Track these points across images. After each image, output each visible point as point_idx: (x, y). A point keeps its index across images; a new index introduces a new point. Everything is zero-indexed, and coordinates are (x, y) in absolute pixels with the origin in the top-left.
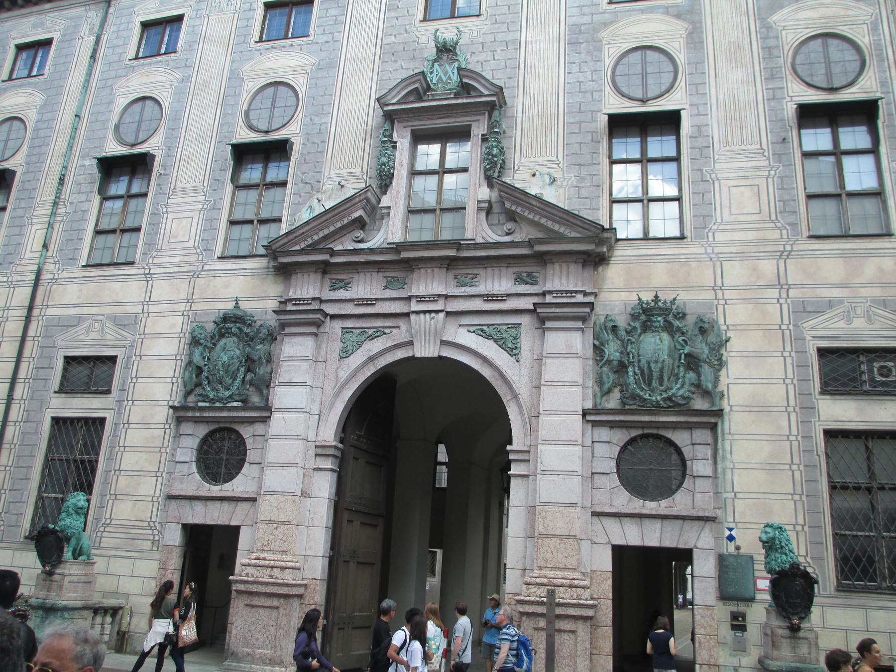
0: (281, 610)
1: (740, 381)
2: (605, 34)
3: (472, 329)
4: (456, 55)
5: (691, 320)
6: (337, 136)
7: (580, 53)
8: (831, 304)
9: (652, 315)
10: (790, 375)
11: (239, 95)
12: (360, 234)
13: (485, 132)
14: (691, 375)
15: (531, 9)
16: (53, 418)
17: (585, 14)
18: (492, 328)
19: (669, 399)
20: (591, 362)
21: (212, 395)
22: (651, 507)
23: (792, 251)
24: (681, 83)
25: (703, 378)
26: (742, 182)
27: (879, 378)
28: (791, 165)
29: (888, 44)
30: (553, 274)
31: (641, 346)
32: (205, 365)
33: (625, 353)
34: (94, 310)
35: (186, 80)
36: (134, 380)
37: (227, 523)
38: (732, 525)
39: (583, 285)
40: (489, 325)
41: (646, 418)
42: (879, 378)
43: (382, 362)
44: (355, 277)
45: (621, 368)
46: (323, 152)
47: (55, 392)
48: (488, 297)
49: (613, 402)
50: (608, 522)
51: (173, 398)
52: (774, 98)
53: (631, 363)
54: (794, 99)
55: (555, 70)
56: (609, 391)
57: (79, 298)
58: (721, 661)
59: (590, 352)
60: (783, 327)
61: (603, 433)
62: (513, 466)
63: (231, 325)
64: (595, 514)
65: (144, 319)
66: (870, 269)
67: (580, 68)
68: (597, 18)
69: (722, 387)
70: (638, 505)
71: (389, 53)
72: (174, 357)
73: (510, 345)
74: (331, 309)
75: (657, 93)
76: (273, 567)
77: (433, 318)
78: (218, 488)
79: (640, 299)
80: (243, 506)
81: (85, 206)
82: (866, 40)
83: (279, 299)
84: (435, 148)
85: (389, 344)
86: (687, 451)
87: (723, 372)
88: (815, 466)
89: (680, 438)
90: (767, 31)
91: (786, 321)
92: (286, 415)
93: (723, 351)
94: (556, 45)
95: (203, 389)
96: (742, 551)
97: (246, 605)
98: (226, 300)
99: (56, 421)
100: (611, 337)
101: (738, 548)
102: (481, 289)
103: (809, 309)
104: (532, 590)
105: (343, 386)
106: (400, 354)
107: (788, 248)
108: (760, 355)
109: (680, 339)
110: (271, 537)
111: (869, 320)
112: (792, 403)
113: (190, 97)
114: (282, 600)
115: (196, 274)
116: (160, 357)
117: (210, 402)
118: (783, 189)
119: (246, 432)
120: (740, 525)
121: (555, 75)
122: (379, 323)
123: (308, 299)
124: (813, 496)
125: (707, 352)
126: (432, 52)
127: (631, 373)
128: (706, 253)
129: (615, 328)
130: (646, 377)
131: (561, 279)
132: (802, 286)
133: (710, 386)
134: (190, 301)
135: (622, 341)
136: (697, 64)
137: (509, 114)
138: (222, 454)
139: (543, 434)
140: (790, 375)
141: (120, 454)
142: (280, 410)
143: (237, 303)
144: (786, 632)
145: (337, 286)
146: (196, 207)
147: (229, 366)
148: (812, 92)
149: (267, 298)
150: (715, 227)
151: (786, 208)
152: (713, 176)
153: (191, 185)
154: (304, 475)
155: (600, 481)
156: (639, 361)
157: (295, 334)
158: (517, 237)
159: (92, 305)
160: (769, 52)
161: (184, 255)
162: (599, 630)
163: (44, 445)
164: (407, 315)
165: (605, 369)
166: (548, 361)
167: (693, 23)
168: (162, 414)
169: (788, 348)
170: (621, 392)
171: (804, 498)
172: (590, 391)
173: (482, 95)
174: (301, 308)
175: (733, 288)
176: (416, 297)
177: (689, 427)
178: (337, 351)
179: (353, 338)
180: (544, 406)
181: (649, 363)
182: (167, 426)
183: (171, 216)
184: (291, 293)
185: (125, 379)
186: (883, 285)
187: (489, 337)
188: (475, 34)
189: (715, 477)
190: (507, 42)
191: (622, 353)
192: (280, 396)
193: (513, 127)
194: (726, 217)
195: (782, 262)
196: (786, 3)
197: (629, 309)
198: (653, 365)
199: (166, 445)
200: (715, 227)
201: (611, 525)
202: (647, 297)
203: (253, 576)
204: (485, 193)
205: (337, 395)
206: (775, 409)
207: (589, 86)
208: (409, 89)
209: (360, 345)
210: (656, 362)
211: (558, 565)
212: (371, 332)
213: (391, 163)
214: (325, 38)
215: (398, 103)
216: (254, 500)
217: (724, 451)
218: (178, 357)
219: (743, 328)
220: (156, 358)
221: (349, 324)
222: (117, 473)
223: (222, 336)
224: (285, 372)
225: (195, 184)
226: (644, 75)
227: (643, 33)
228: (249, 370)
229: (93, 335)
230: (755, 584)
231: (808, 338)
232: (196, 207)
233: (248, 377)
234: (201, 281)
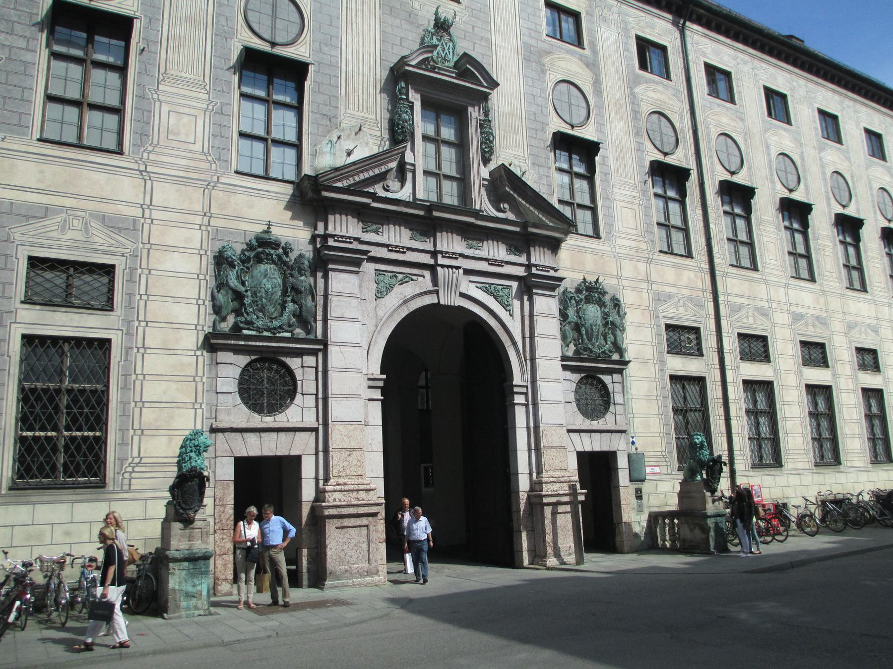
2: (546, 60)
3: (478, 285)
6: (349, 75)
8: (670, 296)
9: (591, 291)
16: (24, 336)
18: (492, 287)
34: (68, 202)
37: (287, 454)
46: (338, 87)
47: (22, 302)
50: (574, 436)
51: (202, 322)
55: (517, 78)
57: (39, 181)
62: (516, 396)
63: (272, 252)
65: (146, 227)
70: (588, 424)
76: (358, 491)
79: (584, 279)
81: (28, 57)
85: (418, 291)
90: (634, 99)
98: (252, 221)
99: (28, 340)
102: (483, 254)
108: (640, 326)
110: (346, 464)
111: (686, 310)
114: (370, 518)
115: (210, 186)
116: (176, 274)
117: (257, 331)
121: (518, 82)
123: (350, 238)
132: (657, 283)
134: (207, 214)
136: (600, 107)
138: (267, 385)
141: (138, 383)
142: (336, 344)
143: (269, 228)
145: (369, 229)
147: (272, 294)
153: (187, 75)
159: (64, 195)
161: (192, 159)
163: (15, 370)
167: (596, 74)
168: (191, 340)
175: (627, 279)
181: (591, 325)
183: (165, 108)
185: (131, 295)
187: (491, 294)
190: (482, 38)
192: (338, 331)
194: (621, 229)
199: (200, 373)
202: (591, 279)
203: (340, 501)
207: (540, 101)
209: (390, 288)
215: (417, 66)
218: (201, 277)
220: (171, 274)
223: (259, 260)
224: (336, 307)
225: (192, 76)
227: (569, 70)
229: (70, 235)
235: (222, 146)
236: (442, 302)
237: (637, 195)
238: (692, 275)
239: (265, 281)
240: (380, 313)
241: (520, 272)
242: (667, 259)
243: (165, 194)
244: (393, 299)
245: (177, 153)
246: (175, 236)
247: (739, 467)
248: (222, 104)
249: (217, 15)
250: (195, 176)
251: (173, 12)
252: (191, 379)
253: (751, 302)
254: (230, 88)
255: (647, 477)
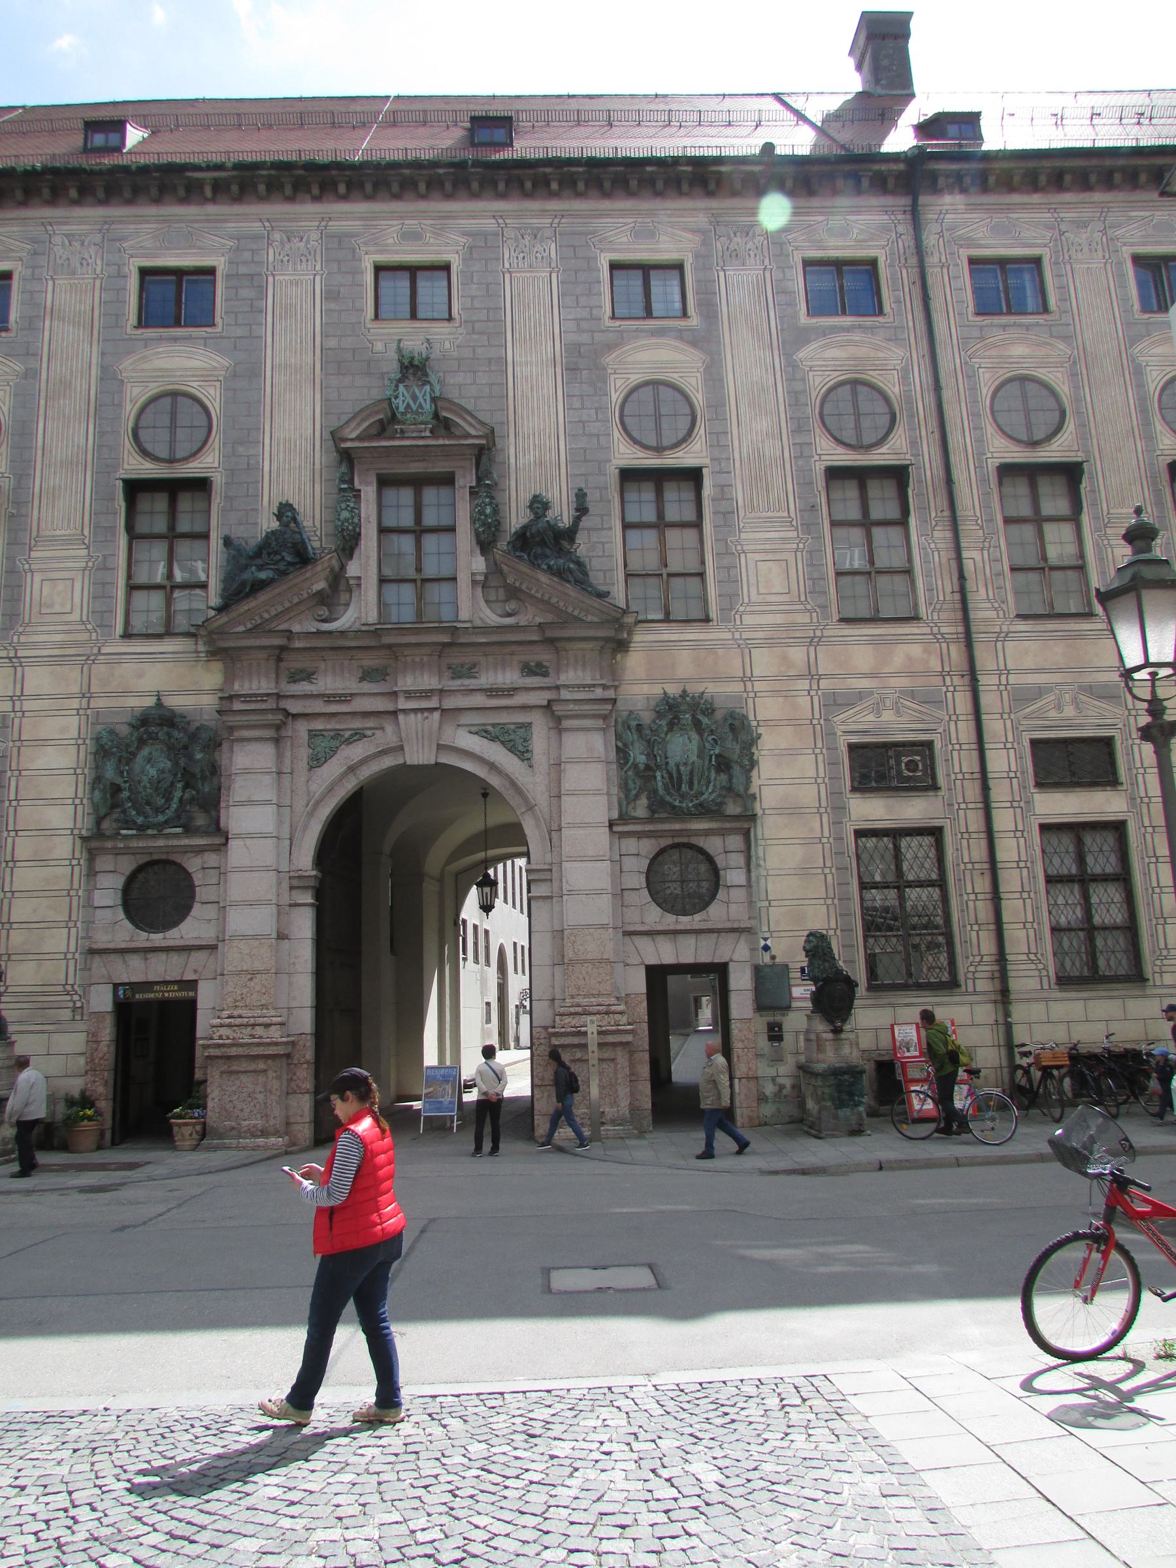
0: (271, 1074)
1: (772, 782)
4: (427, 375)
5: (719, 715)
6: (274, 475)
7: (581, 383)
8: (861, 695)
9: (678, 711)
10: (822, 774)
11: (120, 405)
12: (324, 612)
13: (474, 484)
14: (724, 777)
15: (516, 317)
17: (583, 331)
18: (497, 729)
19: (701, 805)
20: (614, 766)
21: (140, 820)
22: (685, 921)
23: (822, 637)
24: (700, 431)
25: (734, 780)
26: (770, 556)
27: (906, 773)
28: (819, 538)
29: (919, 396)
30: (567, 665)
31: (669, 746)
32: (125, 782)
33: (651, 755)
35: (31, 374)
36: (14, 803)
38: (767, 935)
39: (602, 678)
40: (493, 725)
41: (677, 826)
42: (906, 773)
43: (366, 772)
44: (322, 666)
45: (646, 774)
48: (492, 692)
49: (641, 809)
52: (801, 456)
53: (658, 767)
54: (824, 457)
56: (637, 797)
58: (760, 1073)
59: (613, 755)
60: (815, 722)
61: (630, 845)
64: (627, 934)
65: (17, 721)
66: (900, 655)
67: (582, 404)
68: (598, 337)
69: (754, 789)
71: (335, 363)
72: (72, 771)
73: (521, 748)
74: (294, 707)
75: (674, 441)
76: (254, 1025)
77: (427, 718)
78: (161, 935)
79: (665, 693)
80: (198, 958)
82: (896, 390)
83: (220, 695)
84: (406, 495)
85: (373, 750)
86: (720, 861)
87: (754, 773)
88: (846, 868)
89: (713, 845)
91: (817, 716)
92: (248, 842)
93: (754, 750)
94: (551, 370)
95: (124, 812)
96: (777, 960)
97: (222, 1073)
98: (141, 694)
100: (635, 737)
101: (773, 957)
103: (839, 702)
104: (567, 1021)
105: (318, 803)
106: (388, 762)
107: (818, 633)
109: (710, 738)
110: (245, 991)
111: (898, 713)
112: (824, 804)
113: (42, 402)
114: (269, 1062)
115: (90, 660)
118: (812, 565)
119: (193, 864)
120: (774, 935)
122: (357, 724)
124: (844, 899)
125: (738, 751)
126: (392, 367)
127: (659, 778)
128: (733, 639)
129: (639, 727)
130: (674, 782)
131: (575, 669)
132: (832, 676)
133: (741, 789)
134: (86, 695)
135: (648, 741)
137: (499, 459)
138: (158, 895)
139: (566, 849)
140: (822, 774)
142: (239, 836)
143: (159, 699)
144: (830, 1036)
145: (297, 677)
146: (77, 565)
147: (159, 782)
148: (840, 450)
149: (199, 692)
150: (741, 609)
151: (815, 587)
152: (739, 548)
153: (63, 532)
154: (279, 913)
155: (630, 897)
156: (667, 763)
157: (249, 740)
158: (522, 619)
160: (796, 399)
162: (636, 1056)
164: (394, 713)
165: (630, 773)
166: (568, 766)
168: (64, 847)
169: (819, 745)
170: (648, 798)
171: (836, 901)
172: (615, 799)
173: (468, 436)
174: (253, 706)
175: (763, 679)
176: (405, 692)
177: (722, 833)
178: (305, 760)
179: (322, 744)
180: (565, 820)
181: (678, 766)
182: (75, 862)
183: (38, 578)
184: (236, 687)
186: (911, 674)
188: (447, 345)
189: (749, 885)
191: (648, 755)
193: (505, 475)
194: (754, 597)
195: (812, 649)
196: (813, 337)
197: (653, 703)
198: (682, 768)
199: (76, 886)
200: (741, 609)
201: (644, 944)
202: (673, 690)
204: (479, 564)
205: (311, 814)
206: (808, 810)
208: (372, 420)
209: (335, 751)
210: (685, 764)
211: (592, 992)
212: (347, 734)
213: (356, 520)
214: (239, 332)
215: (359, 438)
216: (214, 948)
217: (758, 858)
219: (773, 724)
220: (43, 772)
221: (319, 725)
222: (7, 926)
223: (142, 742)
226: (658, 417)
227: (655, 362)
228: (187, 786)
230: (790, 993)
231: (839, 733)
232: (77, 565)
233: (187, 796)
234: (99, 669)
235: (104, 609)
236: (408, 763)
237: (795, 534)
238: (916, 650)
239: (148, 767)
240: (314, 787)
241: (540, 698)
242: (857, 632)
243: (38, 679)
244: (333, 769)
245: (52, 628)
246: (50, 727)
247: (1023, 981)
248: (105, 557)
249: (99, 447)
250: (72, 651)
251: (46, 462)
252: (65, 893)
253: (1068, 678)
254: (114, 535)
255: (794, 1004)
